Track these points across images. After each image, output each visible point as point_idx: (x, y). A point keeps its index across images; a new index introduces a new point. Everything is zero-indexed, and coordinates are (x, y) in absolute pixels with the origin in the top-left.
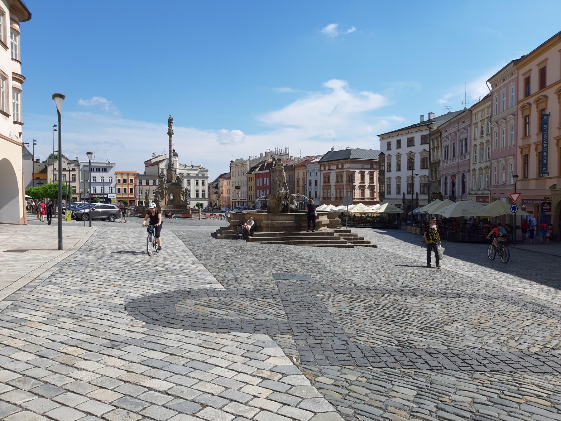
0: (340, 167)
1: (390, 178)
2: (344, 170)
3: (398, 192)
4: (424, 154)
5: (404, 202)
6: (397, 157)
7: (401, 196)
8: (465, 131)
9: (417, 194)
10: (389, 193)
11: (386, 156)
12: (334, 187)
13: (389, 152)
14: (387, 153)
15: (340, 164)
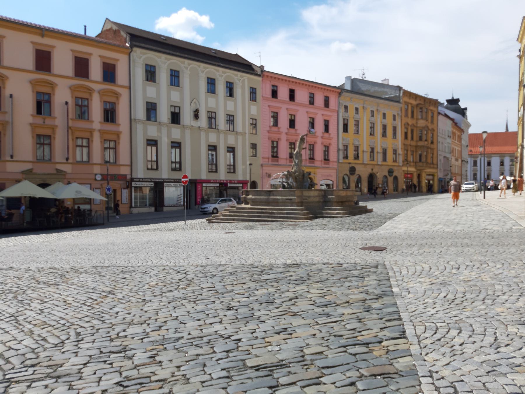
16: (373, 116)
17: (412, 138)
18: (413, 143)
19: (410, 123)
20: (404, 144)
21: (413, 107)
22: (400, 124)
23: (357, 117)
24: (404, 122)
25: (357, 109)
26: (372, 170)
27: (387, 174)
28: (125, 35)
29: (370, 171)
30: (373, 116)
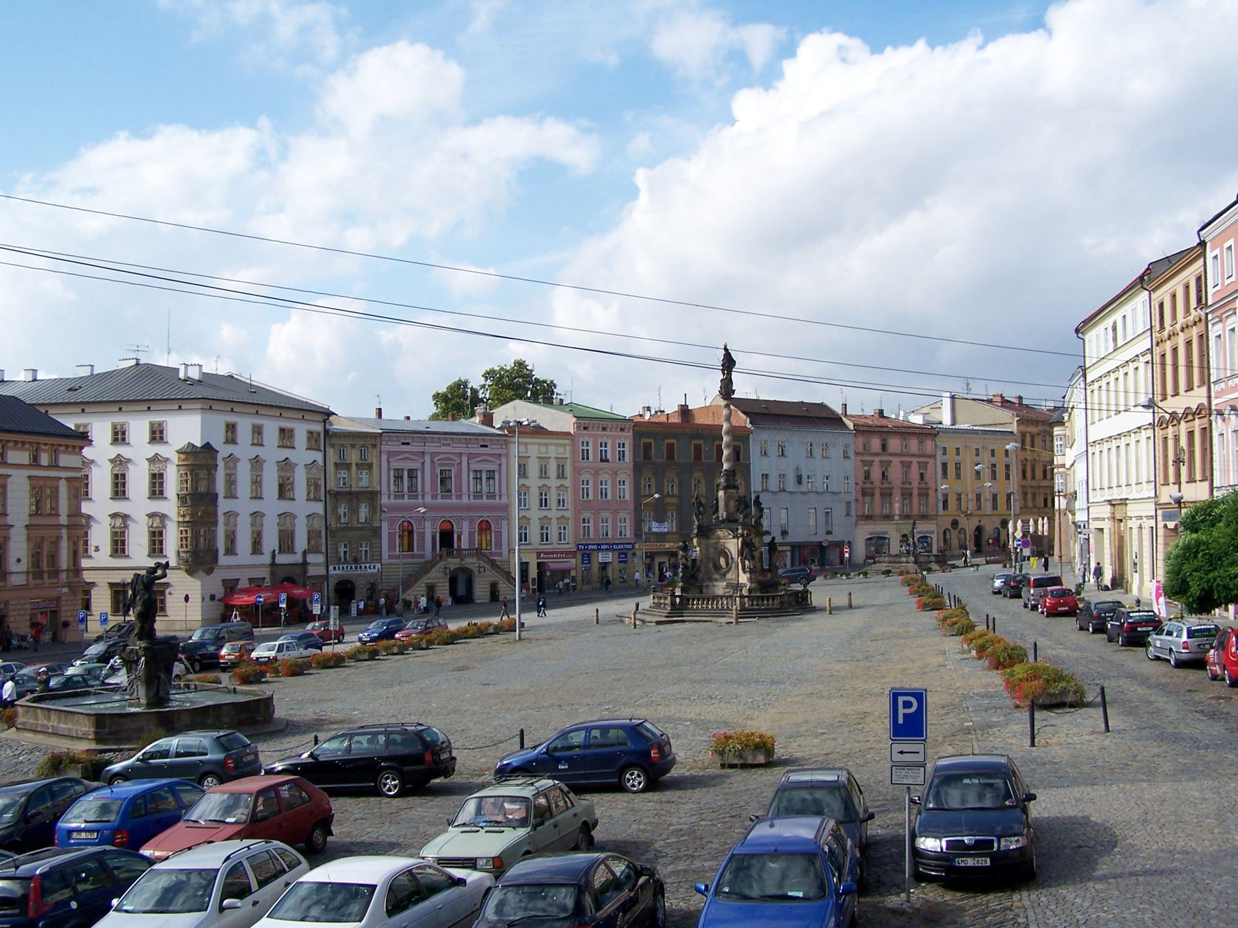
0: (45, 459)
1: (230, 515)
2: (64, 474)
3: (257, 548)
4: (314, 470)
5: (272, 574)
6: (252, 465)
7: (266, 559)
8: (498, 462)
9: (305, 554)
10: (231, 551)
11: (220, 457)
12: (25, 531)
13: (230, 449)
14: (224, 450)
15: (45, 451)
16: (977, 455)
17: (1033, 478)
18: (1034, 483)
19: (1029, 458)
20: (1022, 486)
21: (1032, 437)
22: (1014, 460)
23: (959, 458)
24: (1019, 457)
25: (958, 449)
26: (980, 521)
27: (999, 527)
28: (744, 416)
29: (977, 523)
30: (977, 455)
